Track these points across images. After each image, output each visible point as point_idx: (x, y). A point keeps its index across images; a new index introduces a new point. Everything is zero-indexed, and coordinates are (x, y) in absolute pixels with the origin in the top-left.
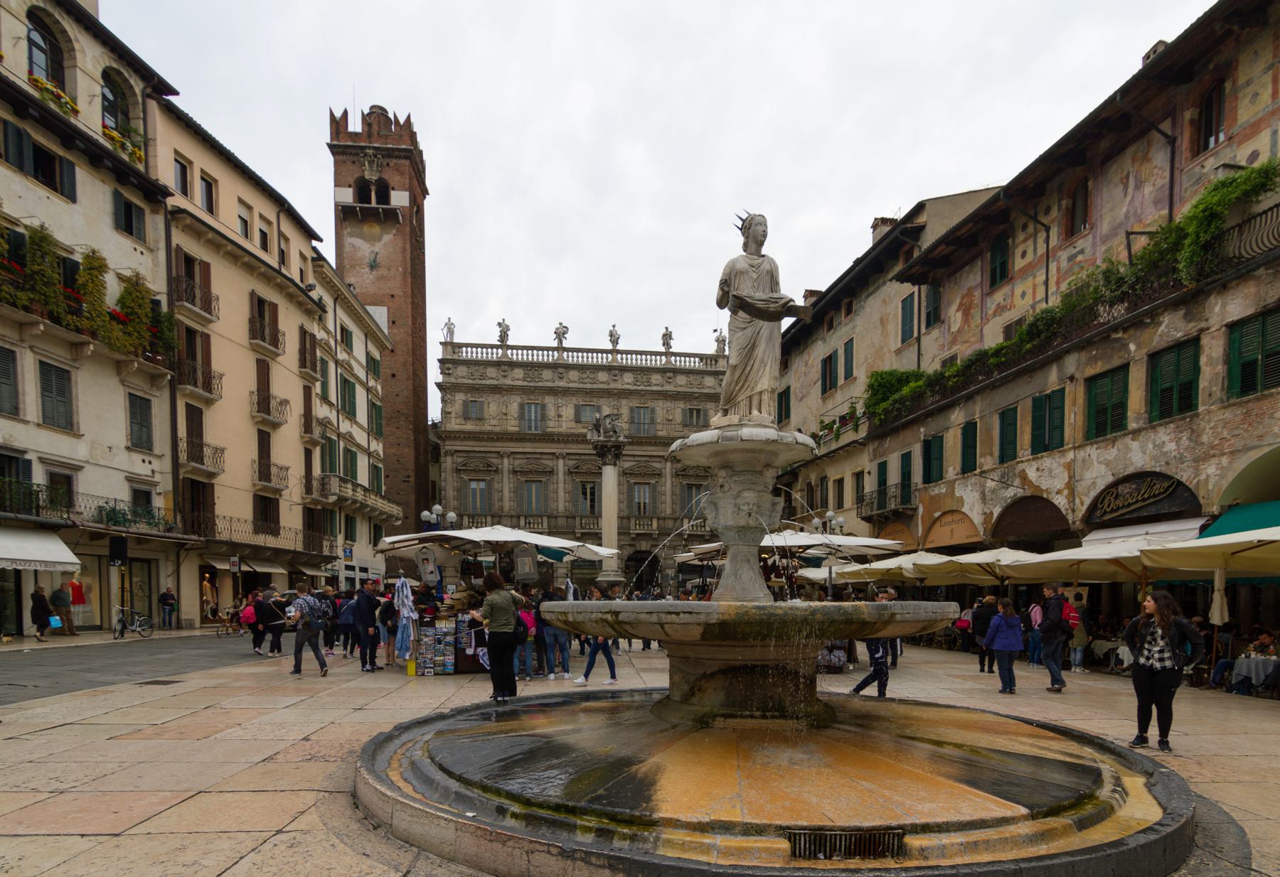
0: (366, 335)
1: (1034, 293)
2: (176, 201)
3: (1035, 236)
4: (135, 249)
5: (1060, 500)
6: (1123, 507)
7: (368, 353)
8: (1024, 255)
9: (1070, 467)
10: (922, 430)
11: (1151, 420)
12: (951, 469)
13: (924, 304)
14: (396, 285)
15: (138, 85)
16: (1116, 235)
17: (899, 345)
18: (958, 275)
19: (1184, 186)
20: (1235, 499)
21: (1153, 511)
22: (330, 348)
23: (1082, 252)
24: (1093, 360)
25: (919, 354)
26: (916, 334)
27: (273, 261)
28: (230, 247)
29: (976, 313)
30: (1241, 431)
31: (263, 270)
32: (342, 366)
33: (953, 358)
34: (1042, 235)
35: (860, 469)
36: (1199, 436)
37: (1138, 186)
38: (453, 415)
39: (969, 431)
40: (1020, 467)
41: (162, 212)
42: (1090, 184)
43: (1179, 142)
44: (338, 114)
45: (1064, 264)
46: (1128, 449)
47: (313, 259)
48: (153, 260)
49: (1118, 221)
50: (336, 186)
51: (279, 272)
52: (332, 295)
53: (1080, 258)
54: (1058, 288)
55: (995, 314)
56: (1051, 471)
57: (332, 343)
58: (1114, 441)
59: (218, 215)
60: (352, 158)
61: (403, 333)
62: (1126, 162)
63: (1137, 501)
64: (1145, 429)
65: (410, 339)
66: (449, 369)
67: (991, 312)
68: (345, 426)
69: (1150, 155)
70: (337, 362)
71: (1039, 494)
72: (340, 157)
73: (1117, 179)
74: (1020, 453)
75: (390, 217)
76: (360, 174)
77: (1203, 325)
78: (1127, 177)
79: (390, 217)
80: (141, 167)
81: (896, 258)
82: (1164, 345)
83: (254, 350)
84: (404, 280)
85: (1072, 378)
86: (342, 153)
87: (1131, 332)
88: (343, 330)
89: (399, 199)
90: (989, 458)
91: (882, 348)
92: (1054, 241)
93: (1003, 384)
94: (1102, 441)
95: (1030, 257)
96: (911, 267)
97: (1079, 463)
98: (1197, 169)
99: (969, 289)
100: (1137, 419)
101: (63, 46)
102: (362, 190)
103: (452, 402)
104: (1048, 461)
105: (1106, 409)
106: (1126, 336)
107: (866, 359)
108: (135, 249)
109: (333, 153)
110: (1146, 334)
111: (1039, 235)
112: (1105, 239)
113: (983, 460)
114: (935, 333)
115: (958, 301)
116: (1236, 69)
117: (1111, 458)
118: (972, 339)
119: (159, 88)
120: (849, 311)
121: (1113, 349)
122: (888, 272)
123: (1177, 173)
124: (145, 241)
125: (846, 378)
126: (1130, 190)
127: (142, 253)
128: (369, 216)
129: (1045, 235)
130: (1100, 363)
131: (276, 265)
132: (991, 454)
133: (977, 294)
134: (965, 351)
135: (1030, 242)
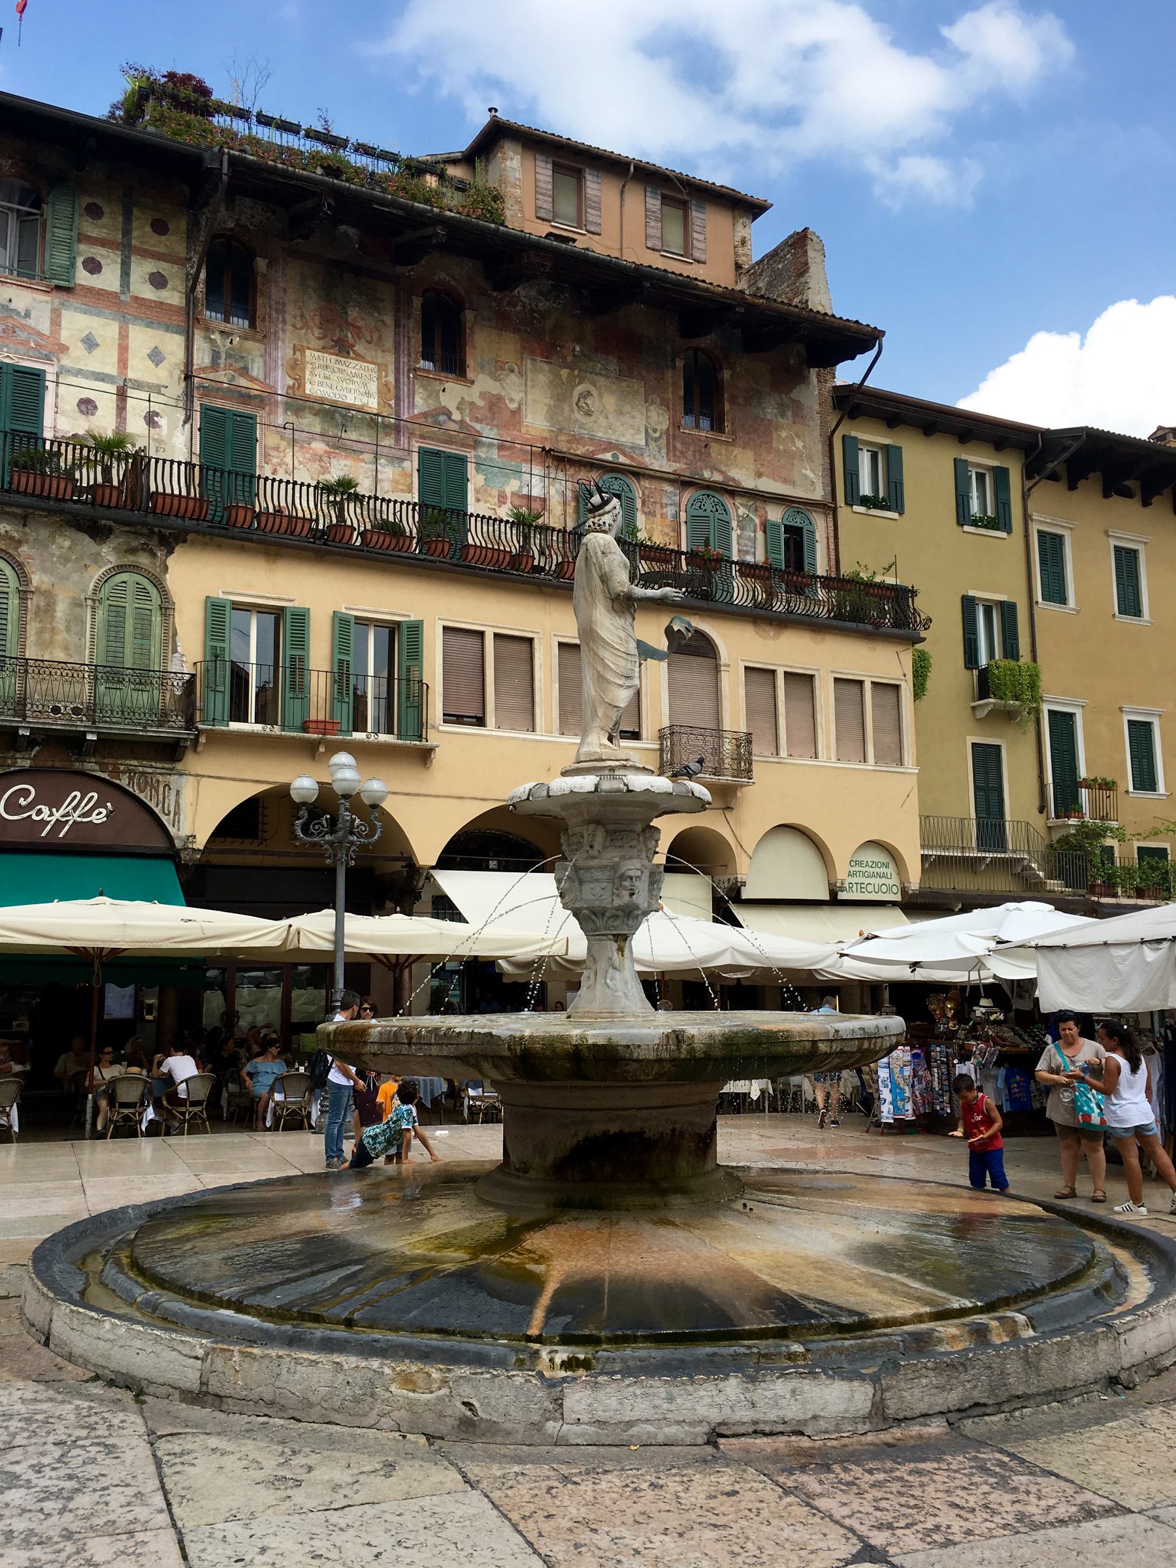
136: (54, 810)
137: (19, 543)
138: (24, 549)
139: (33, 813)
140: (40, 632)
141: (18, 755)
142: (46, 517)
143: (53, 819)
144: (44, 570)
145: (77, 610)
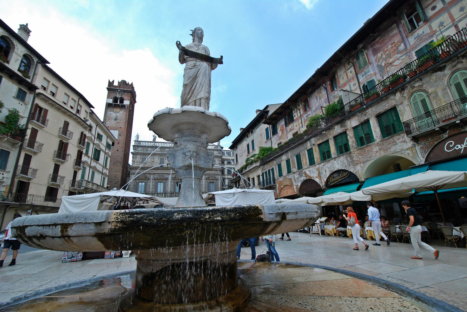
0: (107, 137)
1: (299, 125)
2: (40, 91)
3: (297, 112)
4: (19, 103)
5: (317, 180)
6: (336, 181)
7: (107, 142)
8: (295, 116)
9: (318, 169)
10: (275, 162)
11: (338, 155)
12: (284, 173)
13: (271, 130)
14: (123, 124)
15: (36, 60)
16: (317, 110)
17: (266, 140)
18: (279, 122)
19: (331, 98)
20: (367, 176)
21: (345, 181)
22: (92, 139)
23: (309, 115)
24: (319, 139)
25: (271, 142)
26: (270, 137)
27: (74, 111)
28: (57, 106)
29: (285, 131)
30: (364, 156)
31: (69, 113)
32: (96, 145)
33: (281, 143)
34: (298, 112)
35: (259, 174)
36: (353, 158)
37: (320, 99)
38: (136, 162)
39: (288, 162)
40: (304, 171)
41: (34, 93)
42: (308, 99)
43: (327, 88)
44: (111, 81)
45: (305, 118)
46: (334, 164)
47: (90, 113)
48: (25, 107)
49: (317, 107)
50: (107, 98)
51: (76, 115)
52: (96, 124)
53: (309, 116)
54: (305, 124)
55: (290, 131)
56: (313, 171)
57: (93, 138)
58: (329, 161)
59: (55, 97)
60: (113, 92)
61: (123, 138)
62: (316, 94)
63: (340, 179)
64: (337, 157)
65: (125, 140)
66: (136, 148)
67: (289, 131)
68: (94, 164)
69: (321, 92)
70: (94, 144)
71: (311, 178)
72: (110, 91)
73: (315, 97)
74: (303, 167)
75: (123, 107)
76: (116, 96)
77: (346, 128)
78: (317, 97)
79: (123, 107)
80: (29, 80)
81: (263, 119)
82: (337, 134)
83: (59, 138)
84: (125, 123)
85: (314, 145)
86: (111, 90)
87: (327, 131)
88: (98, 134)
89: (126, 102)
90: (295, 168)
91: (261, 142)
92: (302, 113)
93: (295, 148)
94: (326, 162)
95: (296, 117)
96: (267, 120)
97: (321, 168)
98: (334, 94)
99: (282, 125)
100: (334, 155)
101: (11, 47)
102: (115, 100)
103: (136, 158)
104: (312, 169)
105: (325, 153)
106: (326, 133)
107: (258, 144)
108: (19, 103)
109: (108, 90)
110: (331, 132)
111: (298, 111)
112: (315, 111)
113: (293, 169)
114: (275, 137)
115: (280, 128)
116: (337, 73)
117: (329, 166)
118: (285, 138)
119: (43, 62)
120: (252, 133)
121: (323, 136)
122: (261, 122)
123: (329, 95)
124: (24, 101)
125: (253, 150)
126: (318, 100)
127: (22, 105)
128: (116, 106)
129: (299, 111)
130: (321, 140)
131: (75, 113)
132: (295, 167)
133: (284, 126)
134: (284, 141)
135: (296, 113)
136: (462, 145)
137: (422, 85)
138: (424, 86)
139: (456, 148)
140: (436, 102)
141: (443, 135)
142: (426, 75)
143: (463, 147)
144: (431, 87)
145: (445, 91)
